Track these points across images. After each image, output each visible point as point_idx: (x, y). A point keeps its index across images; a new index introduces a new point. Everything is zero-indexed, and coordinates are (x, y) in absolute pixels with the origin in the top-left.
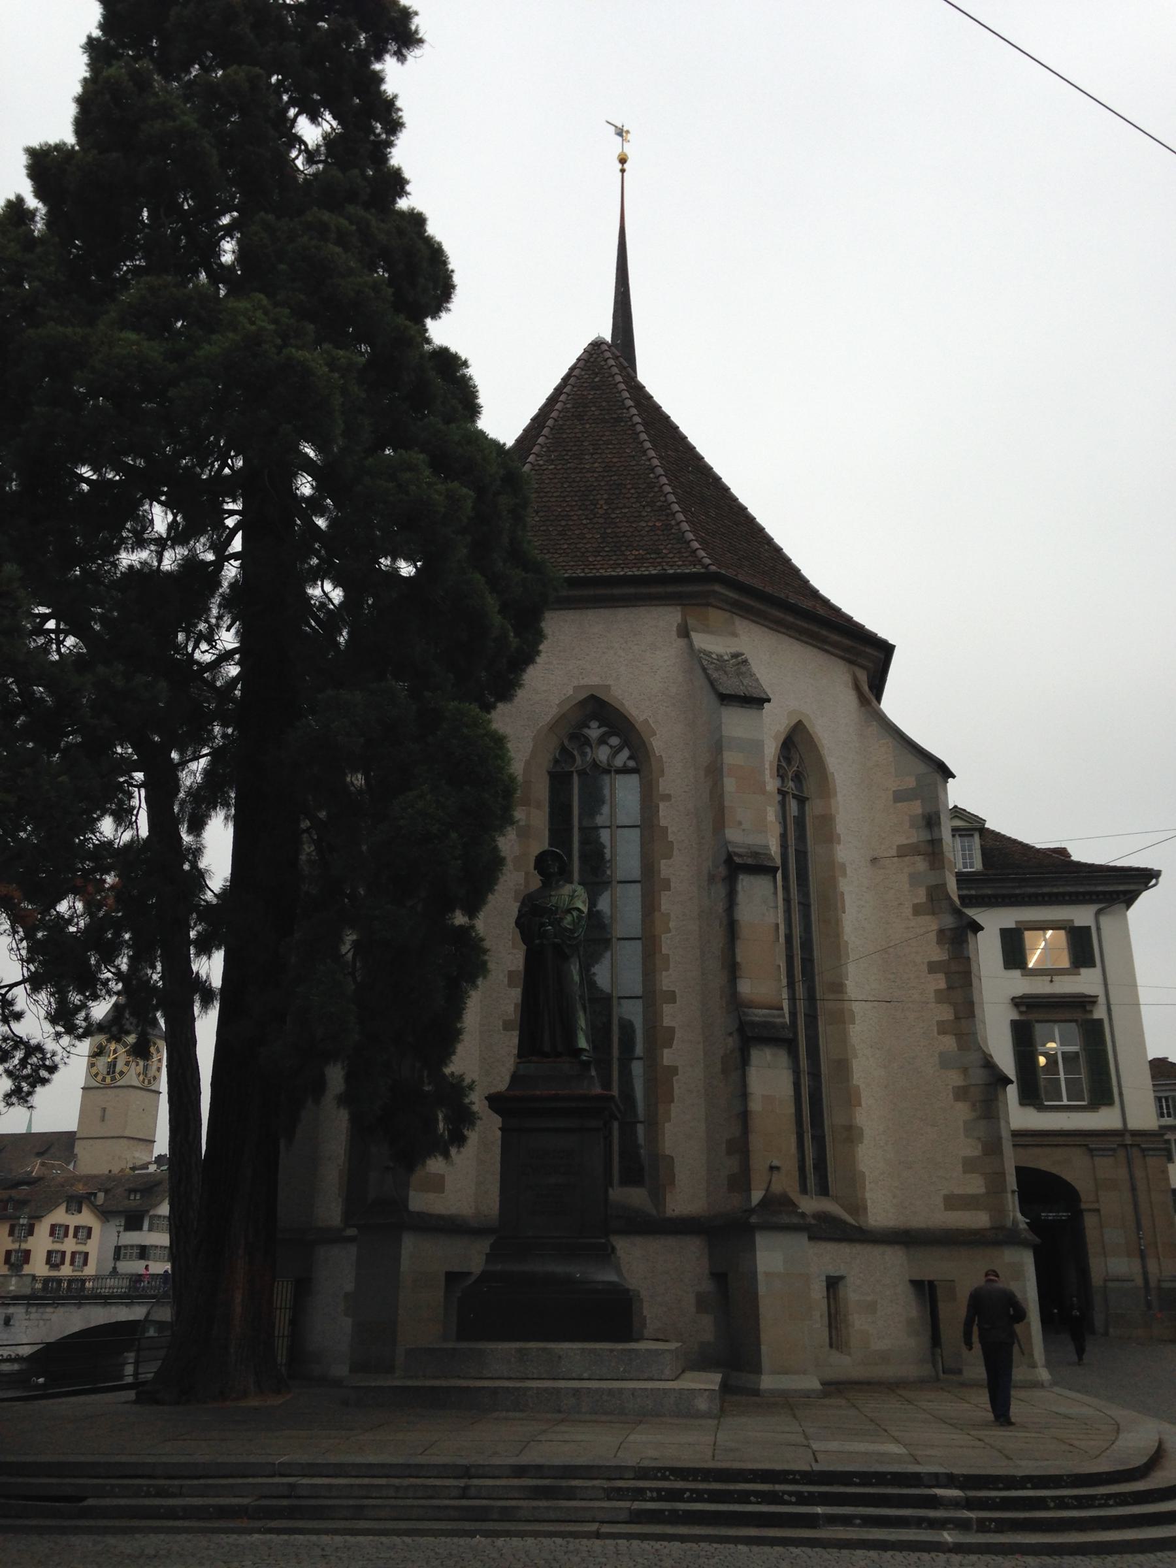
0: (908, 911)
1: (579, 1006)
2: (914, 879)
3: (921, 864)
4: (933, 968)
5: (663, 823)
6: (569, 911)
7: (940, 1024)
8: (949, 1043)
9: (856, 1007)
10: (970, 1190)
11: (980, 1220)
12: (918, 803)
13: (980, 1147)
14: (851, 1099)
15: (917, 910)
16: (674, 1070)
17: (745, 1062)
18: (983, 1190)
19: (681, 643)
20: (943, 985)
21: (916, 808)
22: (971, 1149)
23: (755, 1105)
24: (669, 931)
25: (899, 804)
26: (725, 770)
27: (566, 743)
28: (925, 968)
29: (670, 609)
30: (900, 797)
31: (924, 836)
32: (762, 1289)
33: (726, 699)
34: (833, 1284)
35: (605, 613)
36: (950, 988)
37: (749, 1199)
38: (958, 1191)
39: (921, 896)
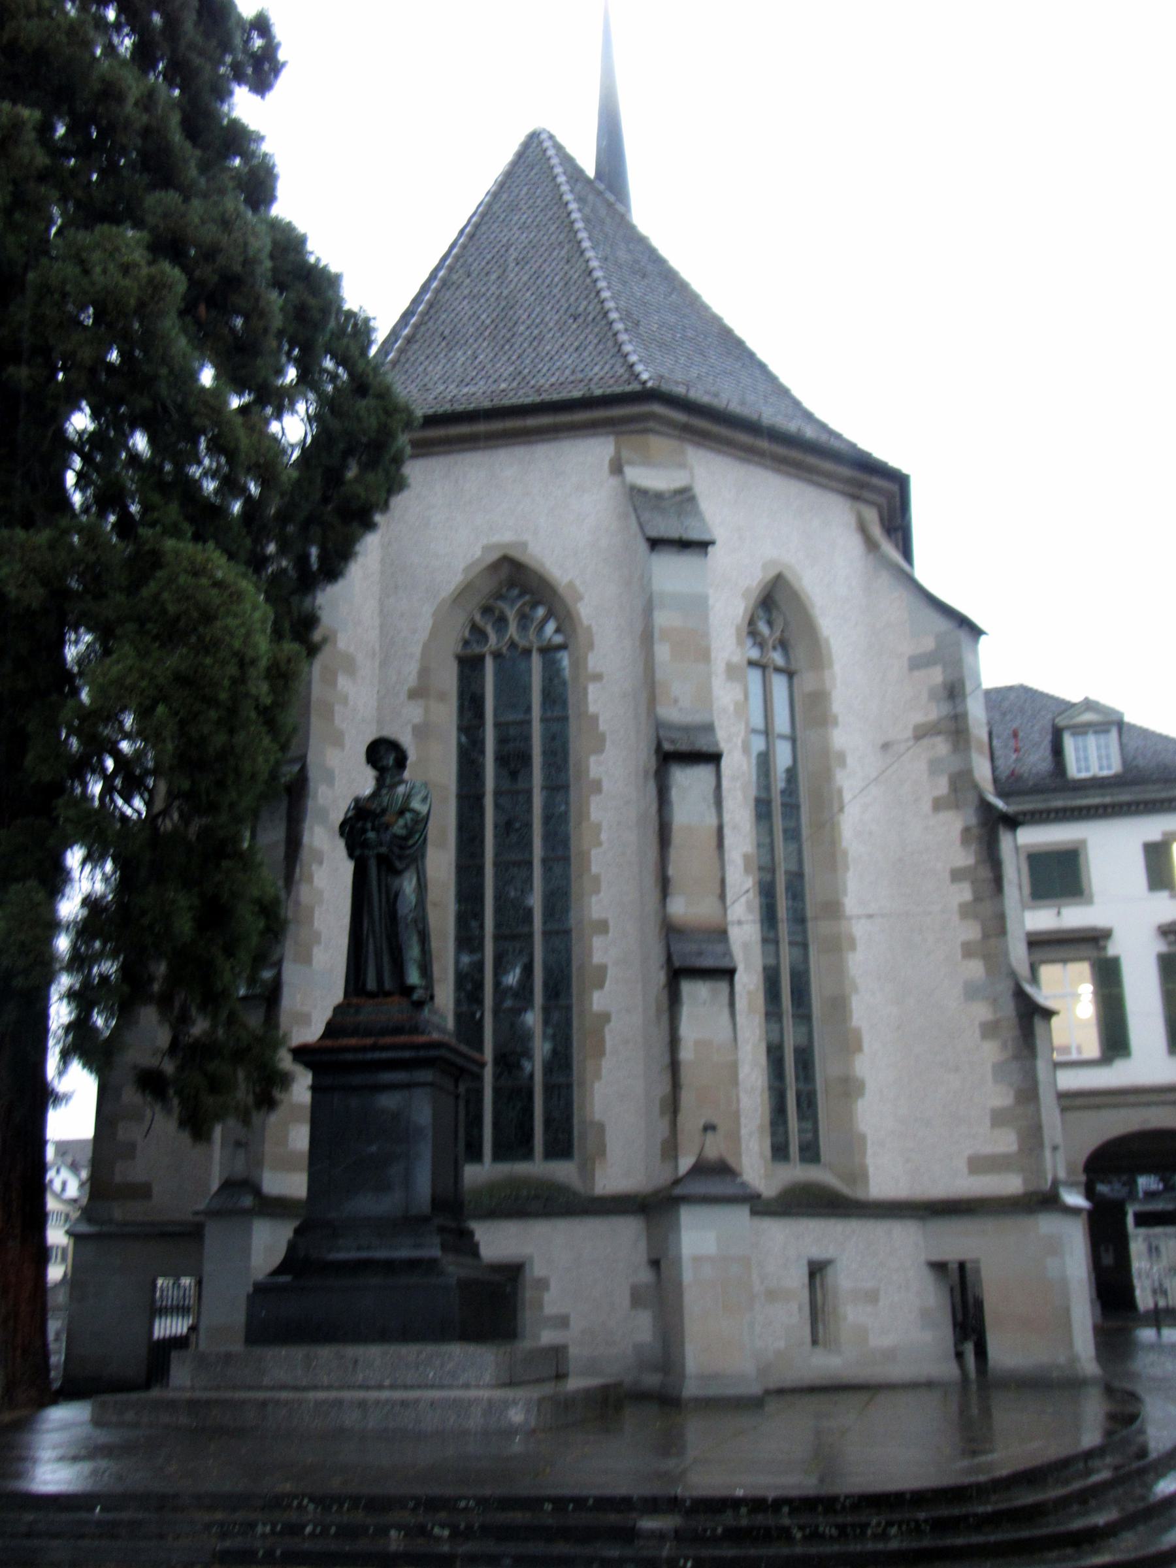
0: (926, 806)
2: (934, 767)
3: (941, 746)
4: (957, 875)
5: (592, 708)
8: (975, 969)
9: (859, 929)
11: (1011, 1184)
13: (1012, 1094)
14: (850, 1044)
15: (938, 805)
17: (674, 999)
18: (1014, 1148)
19: (614, 481)
21: (936, 676)
22: (1001, 1097)
23: (686, 1054)
24: (600, 844)
25: (916, 674)
26: (656, 635)
27: (478, 618)
28: (947, 876)
29: (602, 440)
30: (917, 663)
31: (945, 709)
32: (688, 1276)
33: (655, 544)
34: (817, 1270)
35: (520, 453)
36: (977, 899)
37: (676, 1167)
38: (988, 1149)
39: (942, 786)
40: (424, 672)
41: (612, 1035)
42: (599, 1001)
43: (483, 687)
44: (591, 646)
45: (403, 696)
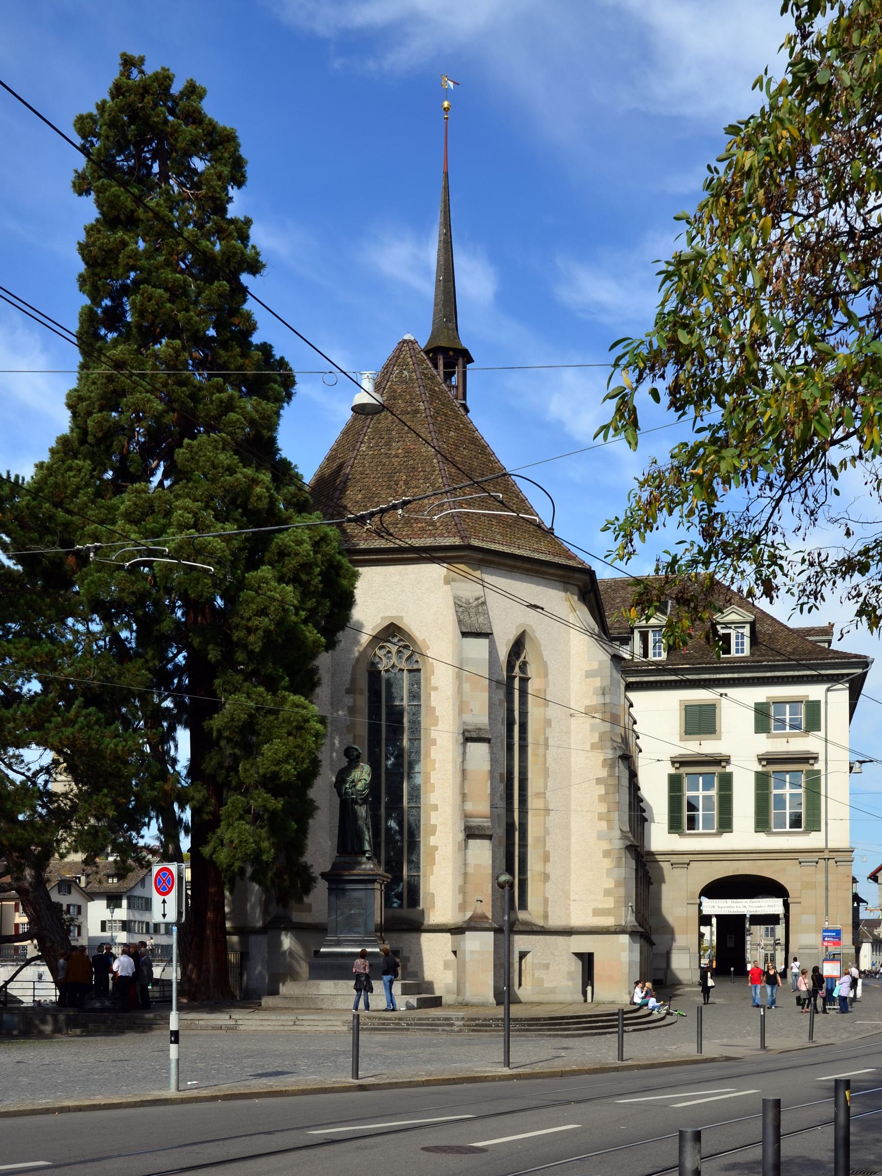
1: (365, 829)
2: (593, 728)
4: (599, 781)
5: (433, 704)
6: (360, 780)
7: (600, 814)
8: (603, 825)
10: (607, 906)
11: (609, 921)
12: (599, 678)
15: (593, 747)
16: (436, 848)
17: (466, 847)
18: (612, 906)
20: (603, 792)
23: (470, 870)
24: (435, 770)
32: (468, 959)
38: (601, 906)
40: (353, 680)
41: (438, 856)
42: (433, 841)
43: (380, 687)
44: (433, 673)
45: (343, 692)
